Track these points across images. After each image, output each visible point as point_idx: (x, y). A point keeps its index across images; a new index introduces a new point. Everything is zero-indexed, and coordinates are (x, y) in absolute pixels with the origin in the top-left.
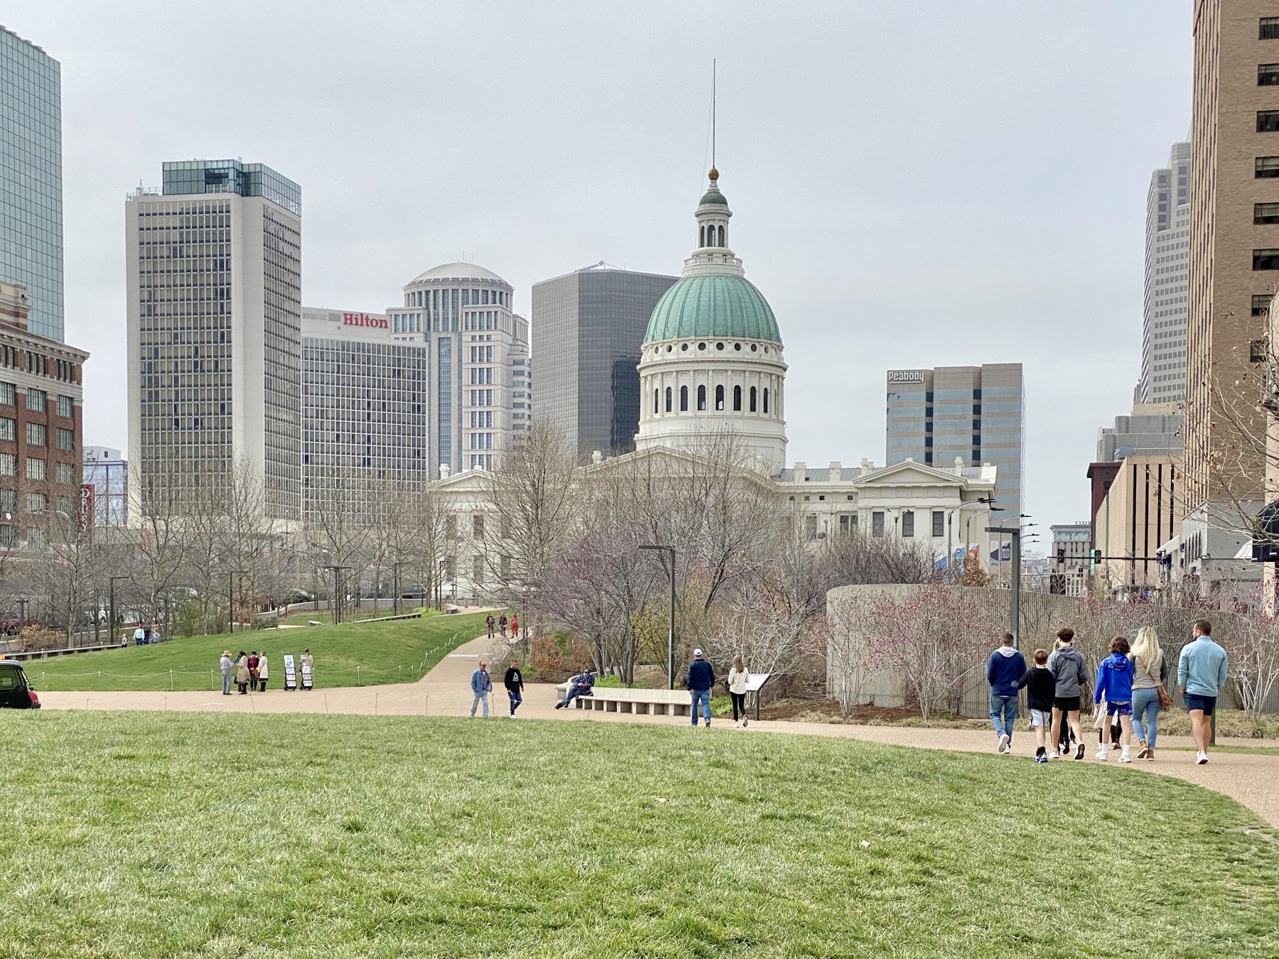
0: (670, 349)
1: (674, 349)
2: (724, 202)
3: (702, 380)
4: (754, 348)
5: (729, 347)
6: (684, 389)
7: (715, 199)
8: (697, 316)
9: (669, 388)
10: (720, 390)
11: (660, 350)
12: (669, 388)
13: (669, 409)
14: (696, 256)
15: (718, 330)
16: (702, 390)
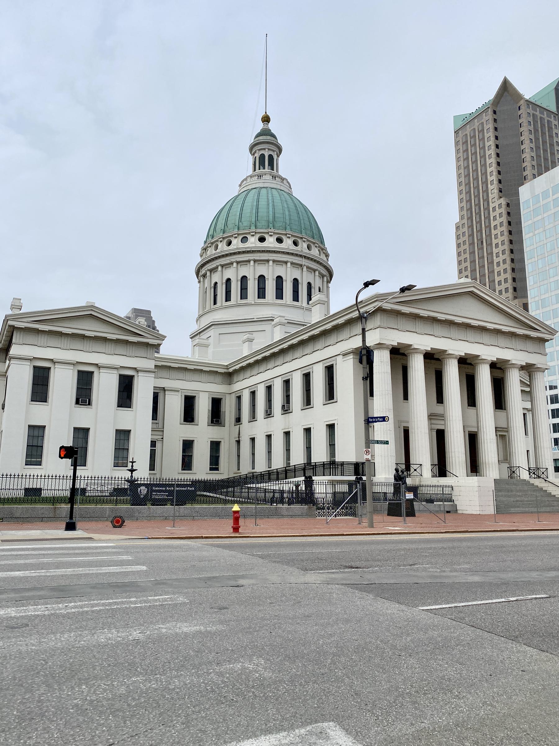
0: (229, 243)
1: (234, 241)
2: (274, 136)
3: (262, 270)
4: (309, 248)
5: (288, 244)
6: (244, 279)
7: (266, 132)
8: (257, 212)
9: (229, 280)
10: (279, 280)
11: (220, 245)
12: (229, 280)
13: (228, 298)
14: (251, 177)
15: (277, 225)
16: (262, 279)
